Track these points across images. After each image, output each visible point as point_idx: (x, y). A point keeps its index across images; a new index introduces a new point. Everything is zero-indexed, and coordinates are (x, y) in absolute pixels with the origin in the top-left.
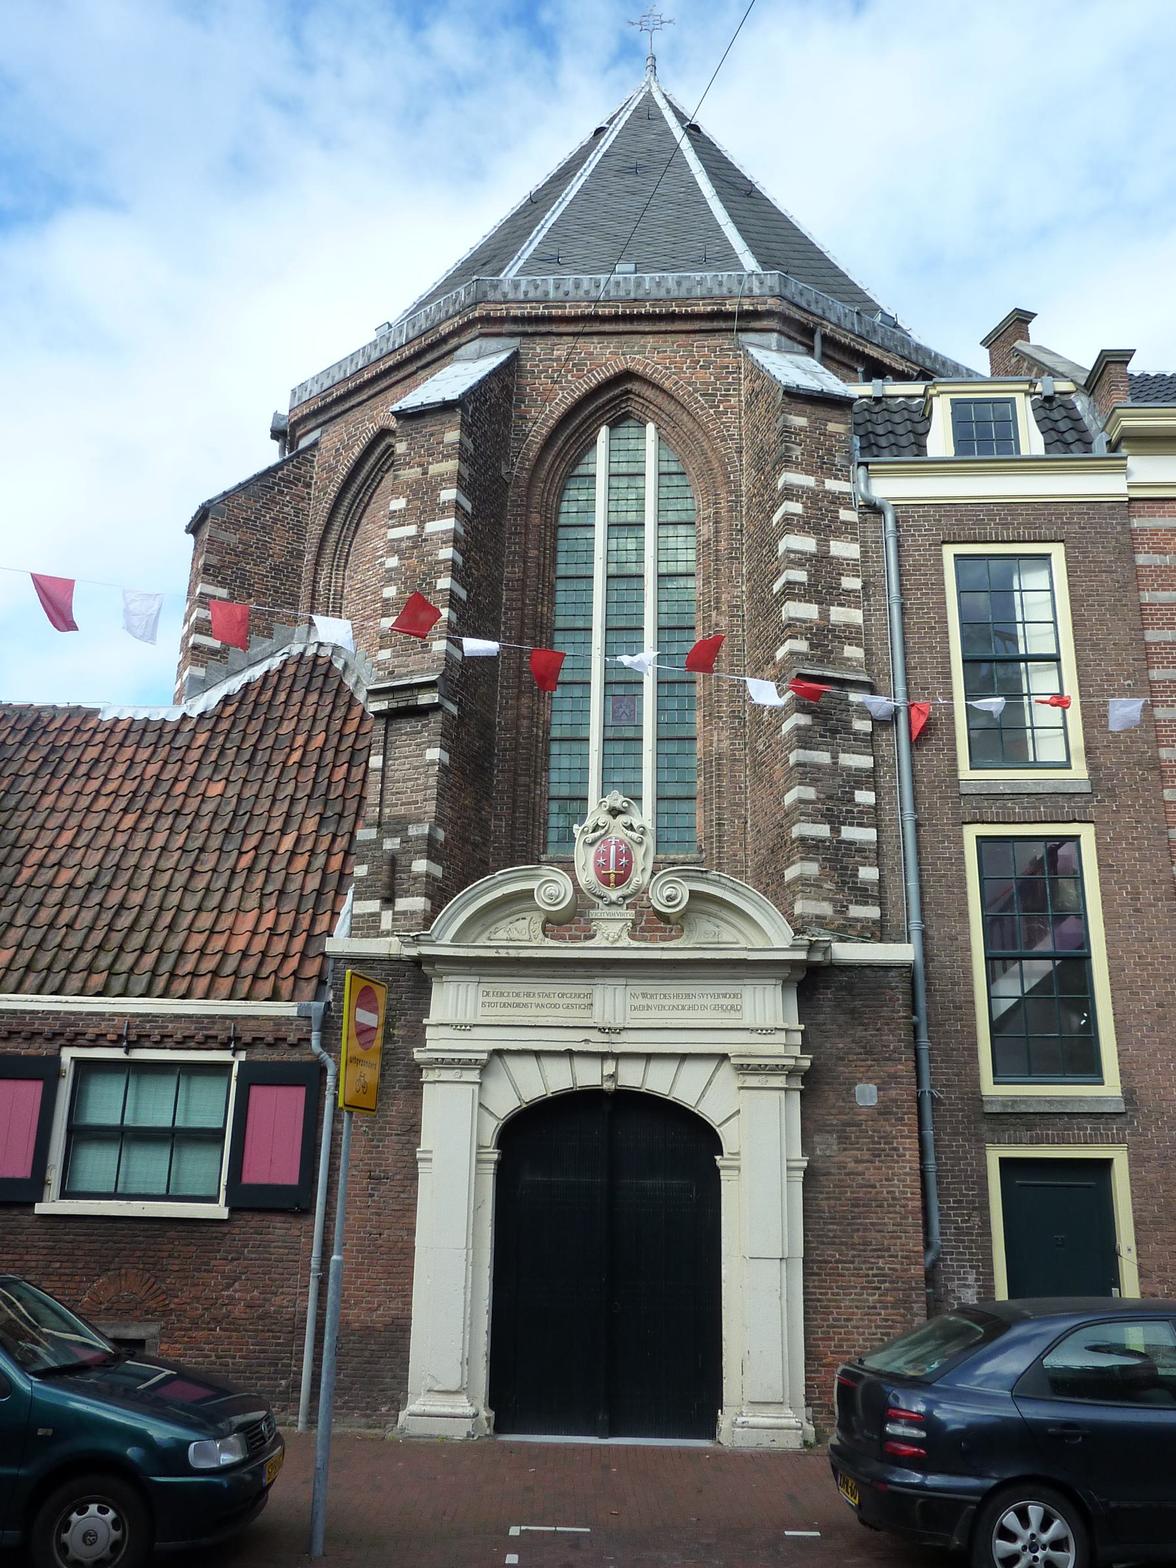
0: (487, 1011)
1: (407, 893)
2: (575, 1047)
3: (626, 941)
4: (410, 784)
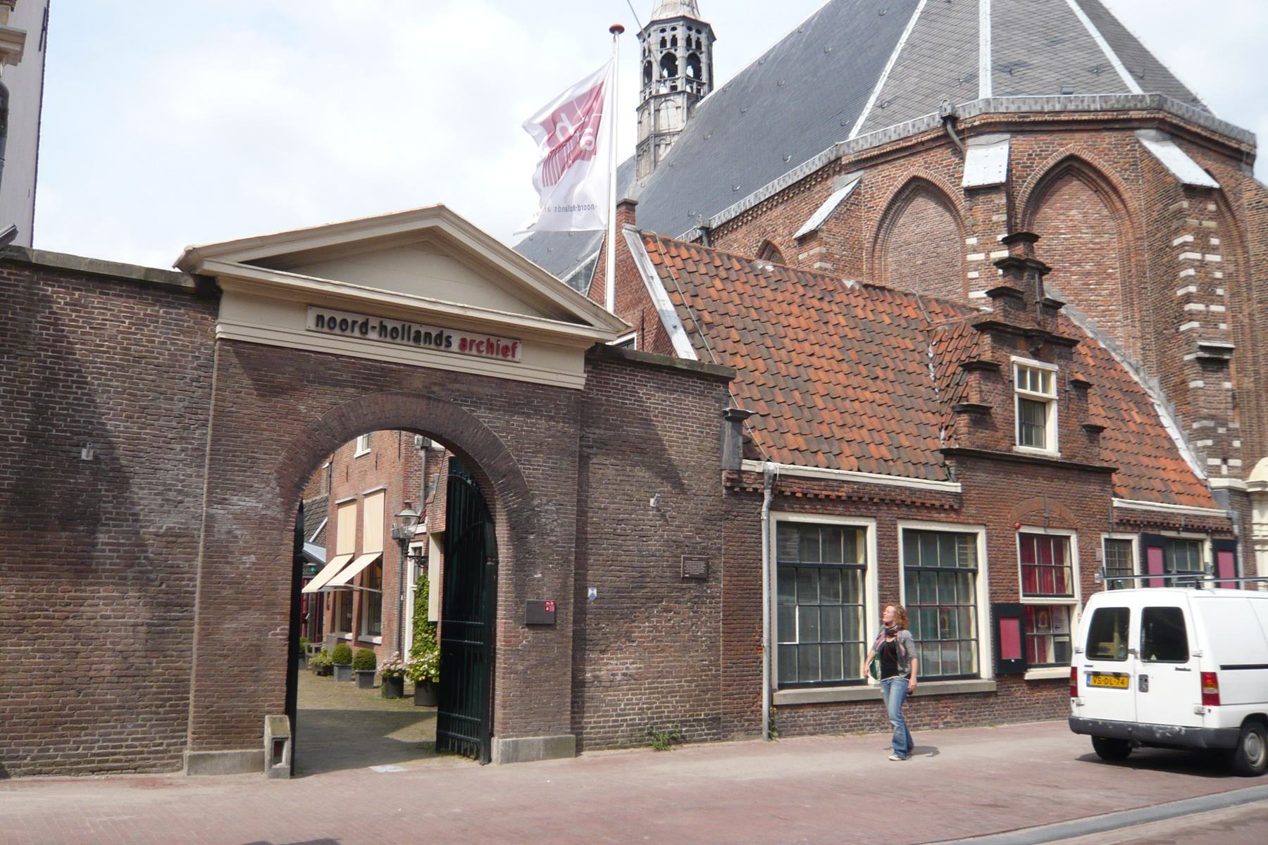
1: (1232, 457)
4: (1216, 398)
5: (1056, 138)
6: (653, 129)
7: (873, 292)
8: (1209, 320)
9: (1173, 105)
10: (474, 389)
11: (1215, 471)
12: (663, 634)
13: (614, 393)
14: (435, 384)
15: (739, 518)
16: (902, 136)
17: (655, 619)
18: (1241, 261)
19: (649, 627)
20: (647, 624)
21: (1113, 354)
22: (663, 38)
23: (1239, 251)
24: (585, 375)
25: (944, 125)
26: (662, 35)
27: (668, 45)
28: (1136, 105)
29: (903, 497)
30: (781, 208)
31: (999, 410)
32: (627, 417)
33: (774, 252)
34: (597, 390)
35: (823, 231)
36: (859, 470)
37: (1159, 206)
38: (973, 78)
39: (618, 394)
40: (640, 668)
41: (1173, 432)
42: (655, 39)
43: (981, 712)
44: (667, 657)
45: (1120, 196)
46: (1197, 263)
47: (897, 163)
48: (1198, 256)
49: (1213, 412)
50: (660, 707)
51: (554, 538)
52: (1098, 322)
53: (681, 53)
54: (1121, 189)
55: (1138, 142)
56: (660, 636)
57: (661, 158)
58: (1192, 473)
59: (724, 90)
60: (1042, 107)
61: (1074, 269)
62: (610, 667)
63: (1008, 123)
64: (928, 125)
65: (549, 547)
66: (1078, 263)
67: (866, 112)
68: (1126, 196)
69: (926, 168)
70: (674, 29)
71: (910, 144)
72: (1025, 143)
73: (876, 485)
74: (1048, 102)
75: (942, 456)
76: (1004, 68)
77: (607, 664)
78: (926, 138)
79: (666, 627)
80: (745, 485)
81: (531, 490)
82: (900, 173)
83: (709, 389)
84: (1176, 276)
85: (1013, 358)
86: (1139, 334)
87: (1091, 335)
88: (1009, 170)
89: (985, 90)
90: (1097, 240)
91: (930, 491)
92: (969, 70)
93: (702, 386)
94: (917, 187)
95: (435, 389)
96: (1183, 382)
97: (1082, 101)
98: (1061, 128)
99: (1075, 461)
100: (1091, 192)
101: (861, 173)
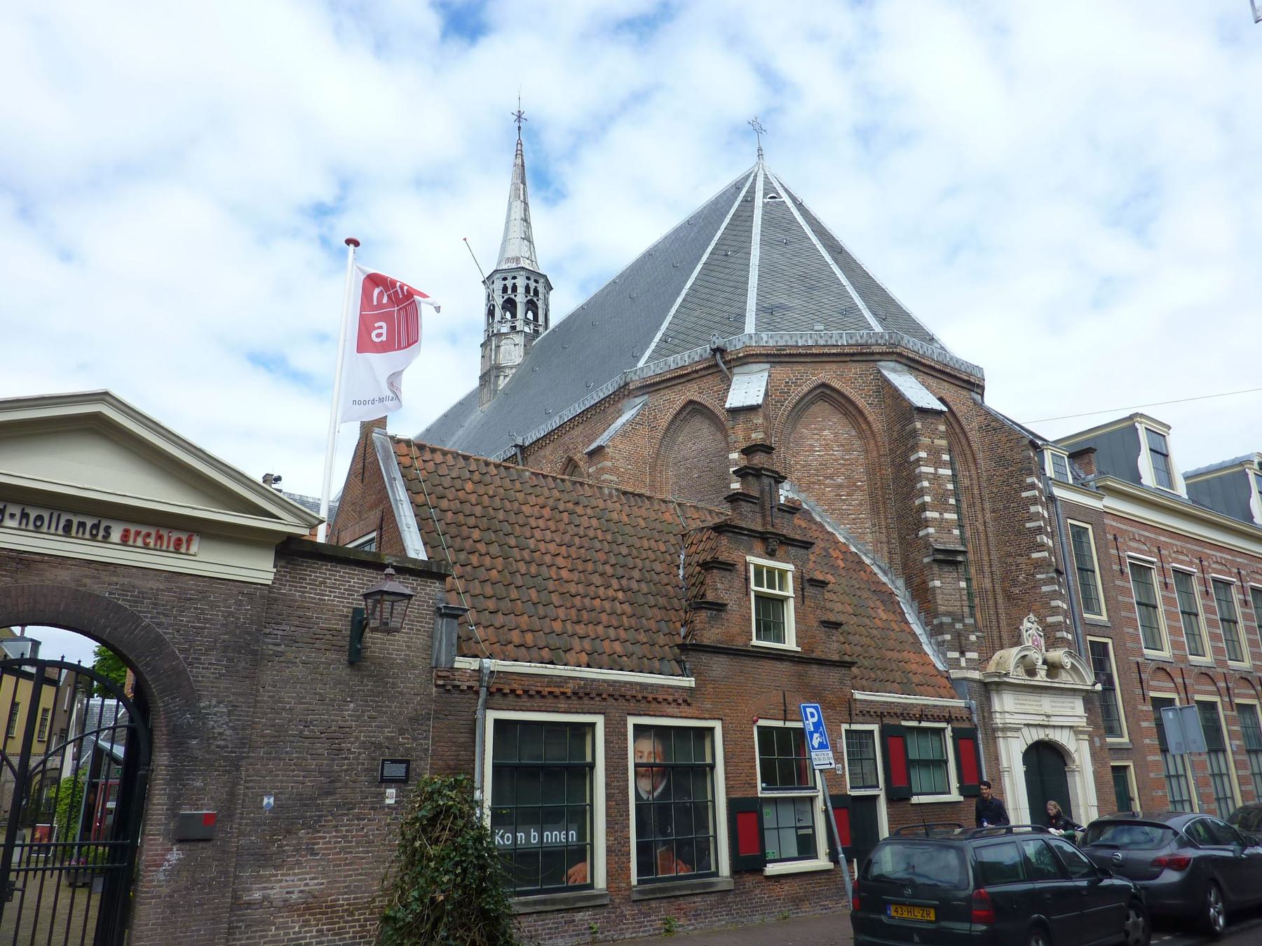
0: (1018, 706)
1: (970, 651)
2: (1041, 723)
3: (1046, 679)
5: (810, 367)
6: (493, 362)
7: (632, 499)
8: (941, 525)
9: (909, 341)
10: (138, 582)
11: (955, 664)
12: (354, 844)
13: (310, 589)
14: (86, 576)
15: (450, 717)
16: (679, 365)
17: (344, 829)
18: (974, 476)
19: (336, 837)
20: (334, 834)
21: (864, 558)
22: (505, 285)
23: (972, 467)
24: (275, 570)
25: (714, 355)
26: (504, 282)
27: (509, 292)
28: (877, 341)
29: (634, 693)
30: (581, 427)
31: (735, 607)
32: (324, 614)
33: (575, 467)
34: (290, 586)
35: (609, 447)
36: (589, 666)
37: (898, 427)
38: (740, 317)
39: (316, 589)
40: (322, 884)
41: (917, 629)
42: (498, 285)
43: (717, 912)
44: (357, 869)
45: (865, 419)
46: (932, 476)
47: (676, 389)
48: (932, 470)
49: (951, 609)
50: (345, 928)
51: (222, 743)
52: (850, 529)
53: (520, 299)
54: (866, 412)
55: (879, 372)
56: (350, 847)
57: (500, 388)
58: (934, 665)
59: (553, 330)
60: (797, 342)
61: (828, 481)
62: (284, 884)
63: (767, 355)
64: (701, 356)
65: (215, 753)
66: (831, 477)
67: (653, 345)
68: (871, 419)
69: (700, 393)
70: (514, 278)
71: (686, 372)
72: (783, 372)
73: (604, 681)
74: (801, 338)
75: (677, 651)
76: (768, 311)
77: (281, 881)
78: (699, 367)
79: (358, 836)
80: (458, 683)
81: (198, 690)
82: (677, 398)
83: (423, 585)
84: (913, 487)
85: (749, 558)
86: (884, 539)
87: (842, 540)
88: (766, 394)
89: (750, 327)
90: (847, 457)
91: (662, 686)
92: (737, 311)
93: (415, 583)
94: (693, 409)
95: (85, 581)
96: (924, 582)
97: (831, 337)
98: (814, 360)
99: (813, 655)
100: (840, 416)
101: (646, 397)
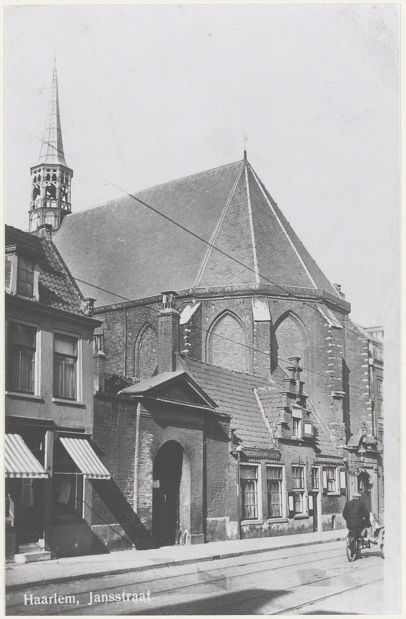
22: (48, 175)
42: (43, 173)
70: (55, 171)
